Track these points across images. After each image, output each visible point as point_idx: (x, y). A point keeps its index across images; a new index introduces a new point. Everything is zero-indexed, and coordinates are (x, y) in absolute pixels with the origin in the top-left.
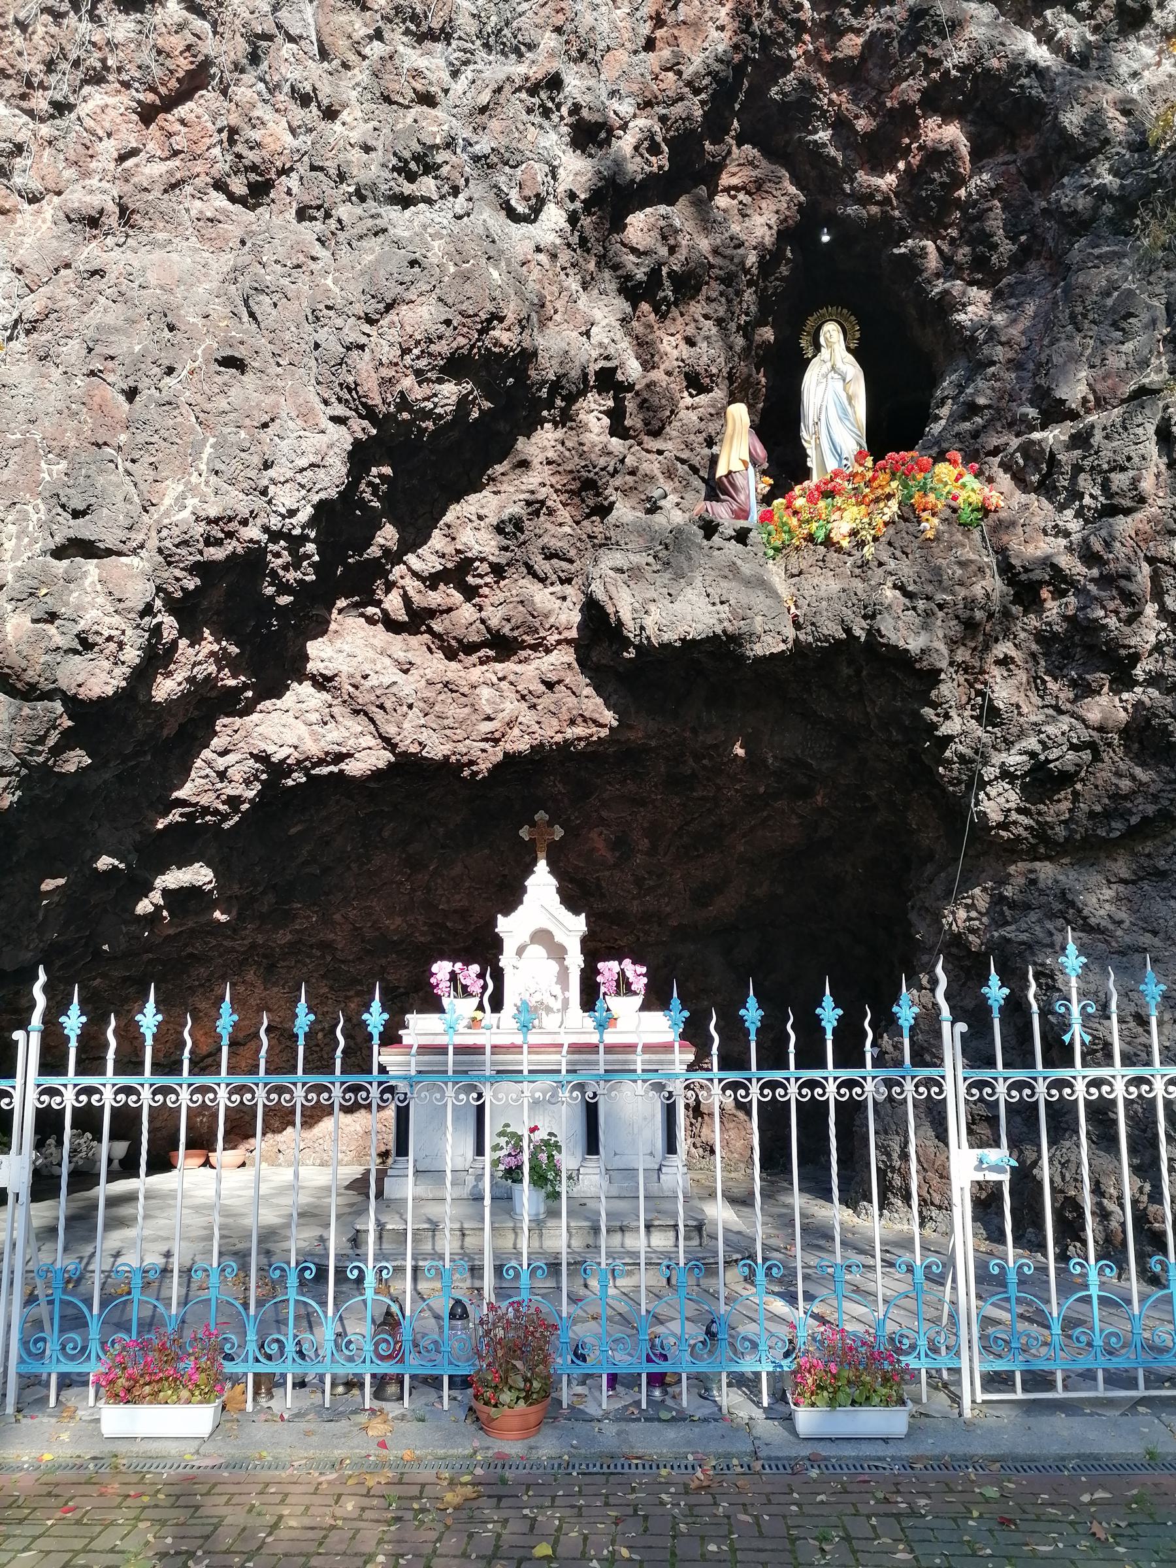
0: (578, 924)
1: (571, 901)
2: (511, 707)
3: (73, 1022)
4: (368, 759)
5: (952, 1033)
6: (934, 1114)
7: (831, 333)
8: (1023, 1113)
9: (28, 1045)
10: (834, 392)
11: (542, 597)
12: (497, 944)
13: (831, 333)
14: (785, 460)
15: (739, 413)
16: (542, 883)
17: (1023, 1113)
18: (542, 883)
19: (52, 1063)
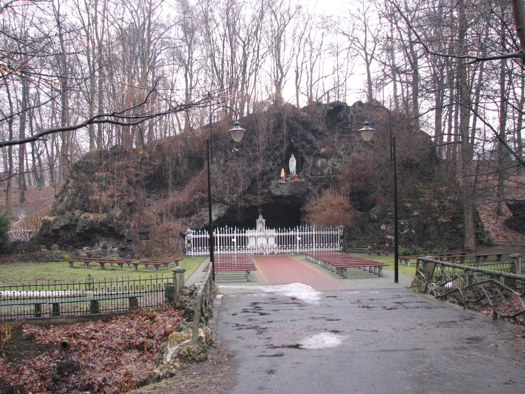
0: (265, 220)
1: (264, 218)
2: (261, 200)
3: (238, 230)
4: (248, 206)
5: (298, 230)
6: (296, 235)
7: (293, 155)
8: (302, 235)
9: (235, 231)
10: (293, 164)
11: (265, 190)
12: (256, 223)
13: (293, 155)
14: (287, 171)
15: (283, 170)
16: (261, 217)
17: (302, 235)
18: (261, 217)
19: (237, 233)
